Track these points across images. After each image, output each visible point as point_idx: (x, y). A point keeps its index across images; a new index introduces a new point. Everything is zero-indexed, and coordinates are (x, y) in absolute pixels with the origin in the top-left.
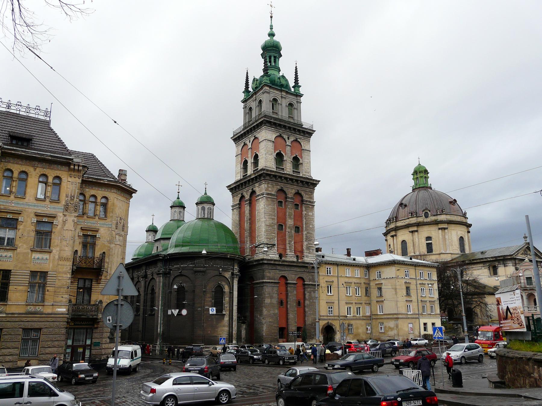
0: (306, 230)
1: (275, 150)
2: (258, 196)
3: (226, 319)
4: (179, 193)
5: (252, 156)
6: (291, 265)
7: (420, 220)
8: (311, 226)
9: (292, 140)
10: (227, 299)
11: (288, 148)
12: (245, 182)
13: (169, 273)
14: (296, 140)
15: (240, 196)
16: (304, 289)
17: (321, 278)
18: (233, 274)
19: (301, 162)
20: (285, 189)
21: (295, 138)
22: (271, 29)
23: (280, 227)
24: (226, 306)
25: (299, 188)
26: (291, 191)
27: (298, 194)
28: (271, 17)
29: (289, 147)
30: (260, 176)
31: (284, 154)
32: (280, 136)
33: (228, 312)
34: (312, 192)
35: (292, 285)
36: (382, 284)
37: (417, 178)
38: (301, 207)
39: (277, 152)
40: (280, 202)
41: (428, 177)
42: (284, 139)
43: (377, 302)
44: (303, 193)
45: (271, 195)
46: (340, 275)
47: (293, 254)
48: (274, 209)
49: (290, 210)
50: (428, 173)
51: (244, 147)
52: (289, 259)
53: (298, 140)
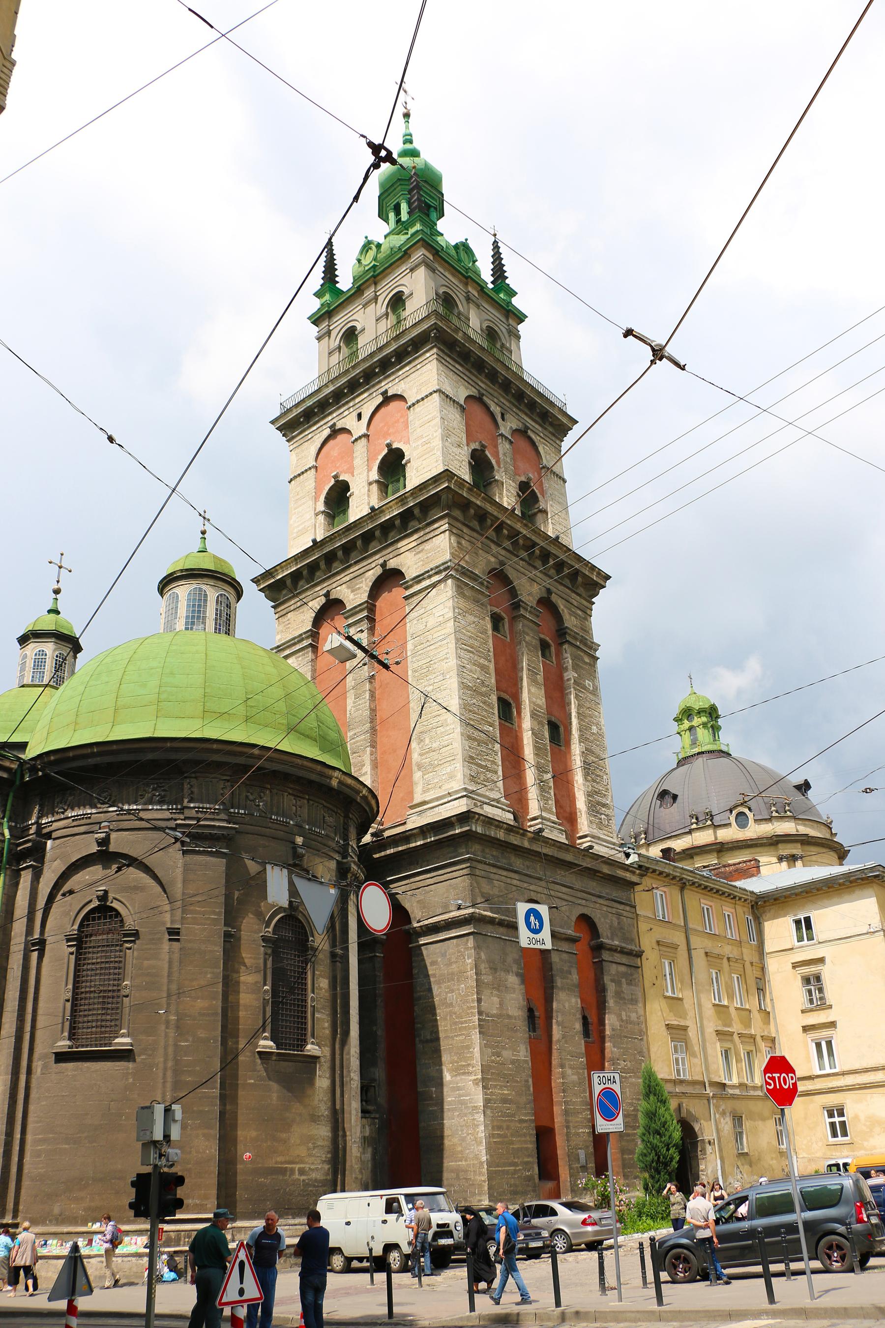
0: (583, 739)
1: (470, 438)
2: (418, 579)
3: (322, 1082)
4: (57, 592)
5: (369, 461)
7: (724, 835)
8: (594, 729)
9: (514, 427)
10: (319, 985)
11: (504, 447)
12: (348, 549)
13: (37, 852)
14: (522, 432)
15: (317, 604)
16: (599, 967)
17: (643, 926)
19: (542, 505)
20: (511, 574)
21: (520, 426)
25: (548, 582)
26: (530, 587)
27: (546, 602)
29: (508, 446)
30: (426, 507)
31: (494, 462)
33: (327, 1051)
34: (586, 613)
36: (821, 960)
37: (691, 729)
38: (559, 654)
40: (496, 621)
41: (719, 728)
42: (492, 416)
43: (806, 1029)
44: (561, 605)
45: (474, 577)
46: (691, 925)
47: (554, 818)
48: (484, 632)
50: (718, 717)
51: (331, 443)
53: (530, 433)
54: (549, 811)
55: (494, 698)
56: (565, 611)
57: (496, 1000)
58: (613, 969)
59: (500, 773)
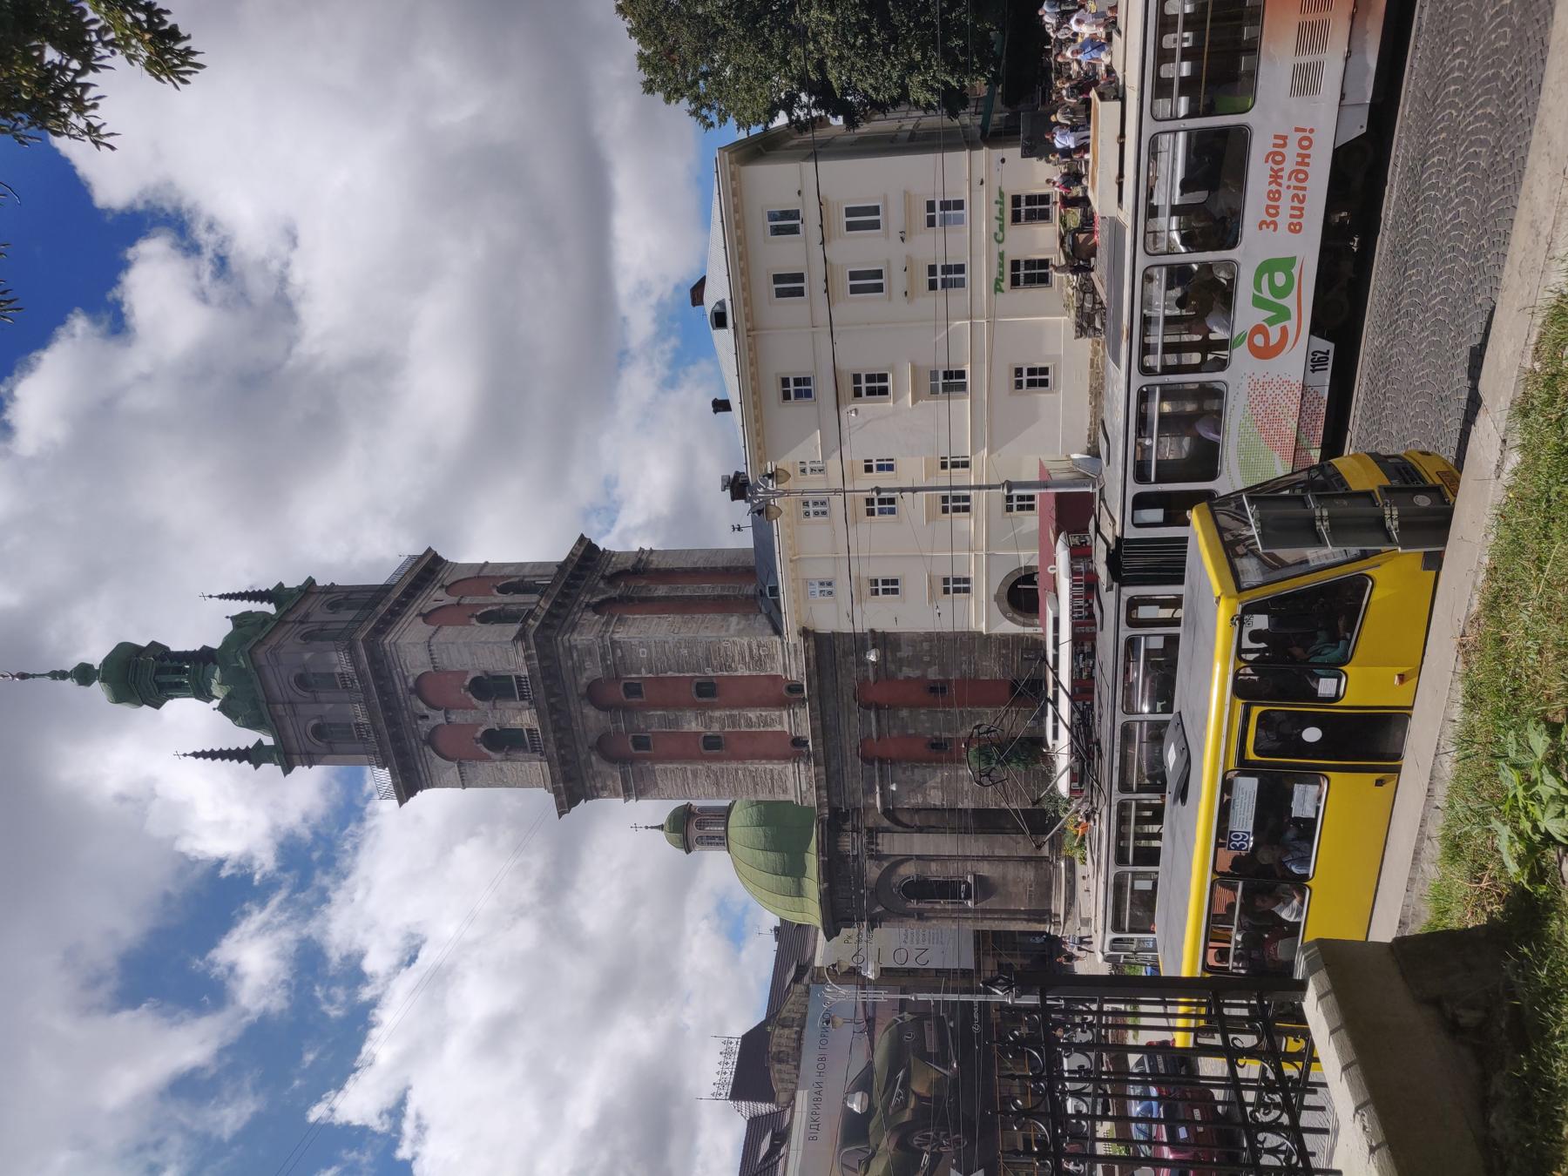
0: (698, 668)
3: (985, 869)
6: (825, 727)
9: (422, 705)
18: (871, 857)
21: (413, 697)
22: (63, 675)
23: (713, 746)
24: (952, 870)
27: (593, 694)
28: (23, 676)
31: (482, 729)
32: (430, 740)
35: (884, 722)
39: (485, 750)
44: (583, 680)
47: (785, 713)
48: (665, 771)
49: (653, 721)
52: (805, 730)
54: (781, 717)
55: (715, 766)
56: (587, 674)
57: (932, 792)
58: (892, 667)
59: (769, 766)
